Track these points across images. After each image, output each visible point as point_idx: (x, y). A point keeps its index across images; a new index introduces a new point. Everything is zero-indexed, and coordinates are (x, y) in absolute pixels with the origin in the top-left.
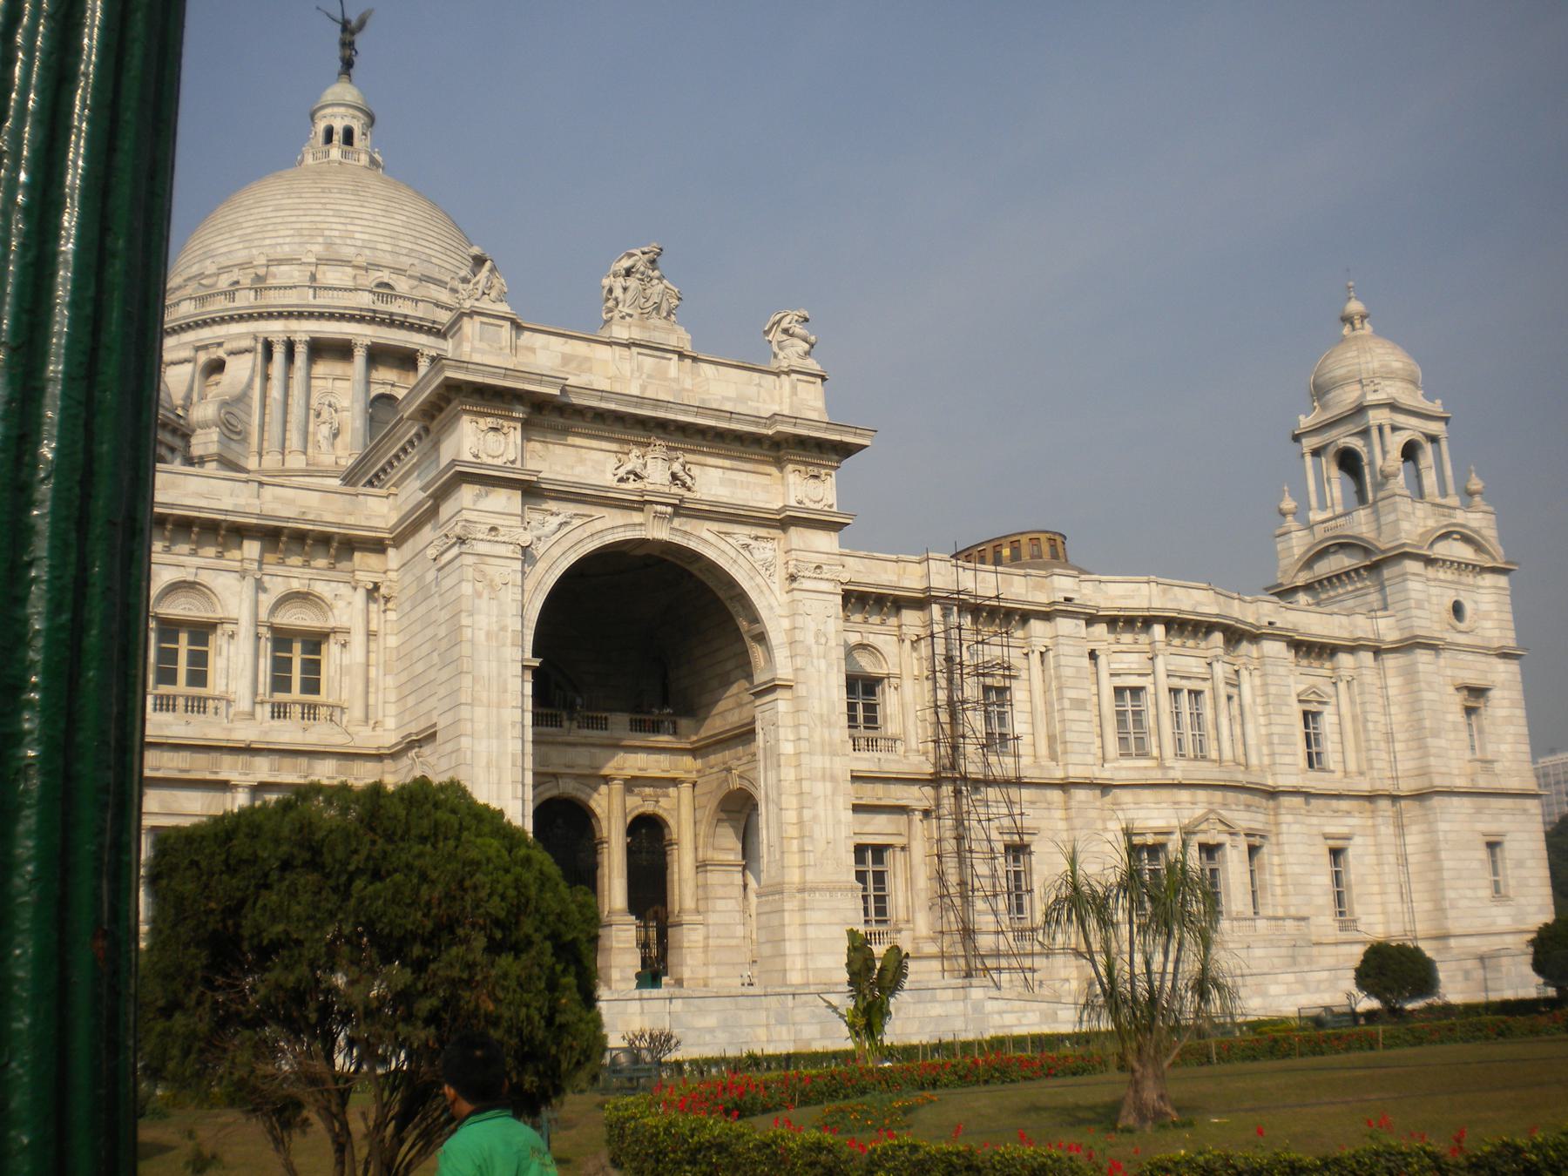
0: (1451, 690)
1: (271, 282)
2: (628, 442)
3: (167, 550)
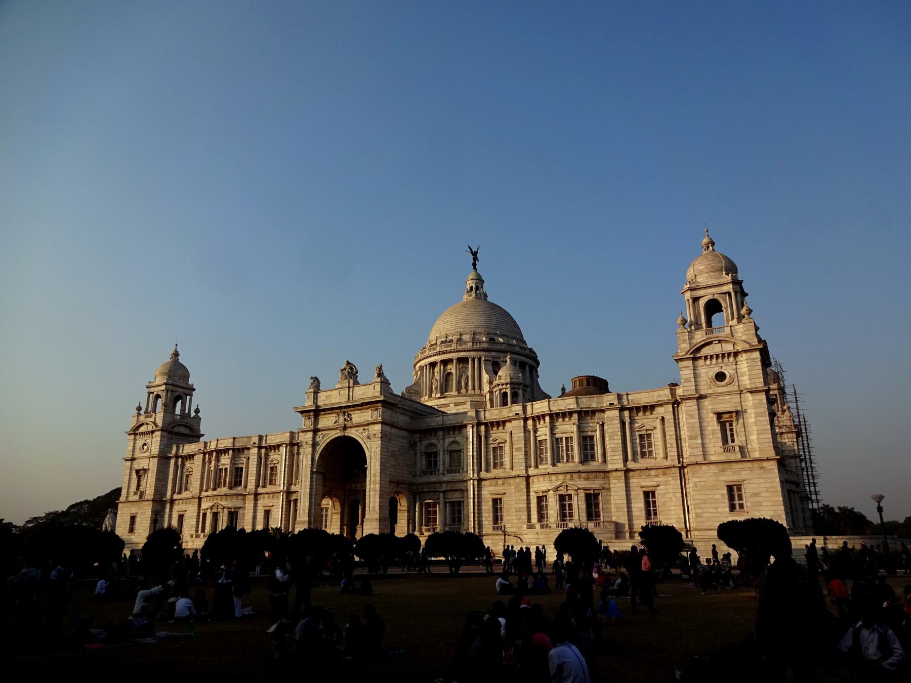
0: (711, 415)
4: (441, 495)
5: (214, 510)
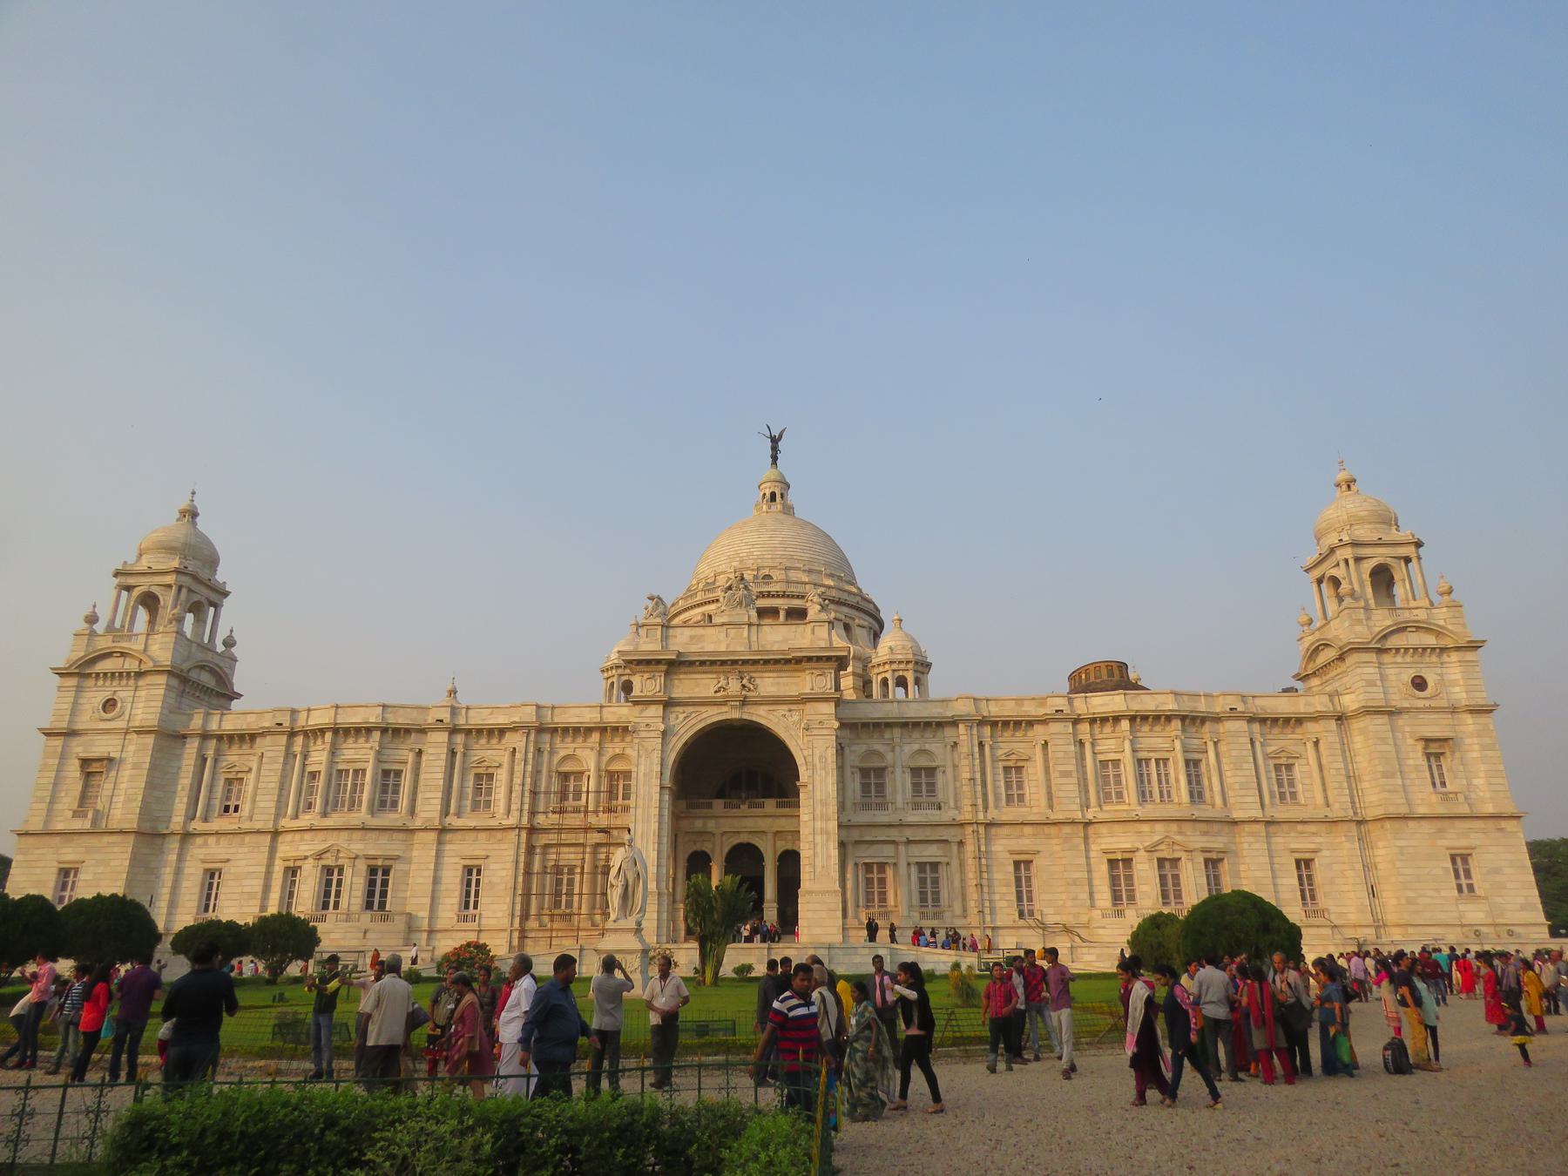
0: (1410, 741)
1: (717, 584)
4: (902, 848)
5: (330, 862)
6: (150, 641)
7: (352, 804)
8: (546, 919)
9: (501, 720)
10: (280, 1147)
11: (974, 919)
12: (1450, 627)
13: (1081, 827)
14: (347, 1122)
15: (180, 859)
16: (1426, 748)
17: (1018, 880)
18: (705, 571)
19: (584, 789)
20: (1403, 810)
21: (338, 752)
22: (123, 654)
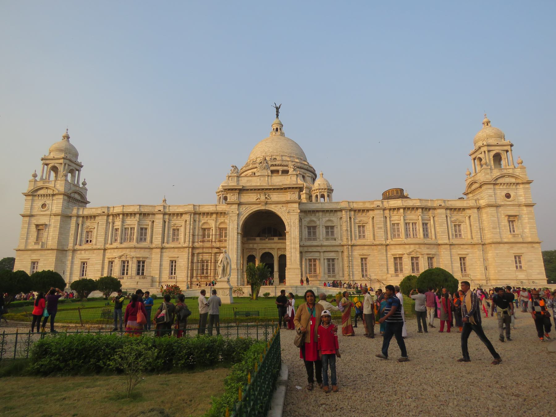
0: (503, 216)
2: (257, 193)
3: (203, 217)
4: (322, 254)
6: (56, 183)
7: (131, 239)
8: (199, 278)
9: (181, 210)
10: (90, 353)
11: (346, 278)
12: (520, 176)
13: (385, 246)
14: (113, 345)
15: (73, 258)
16: (508, 219)
17: (362, 264)
18: (253, 157)
19: (211, 234)
20: (499, 240)
21: (125, 222)
22: (47, 188)
